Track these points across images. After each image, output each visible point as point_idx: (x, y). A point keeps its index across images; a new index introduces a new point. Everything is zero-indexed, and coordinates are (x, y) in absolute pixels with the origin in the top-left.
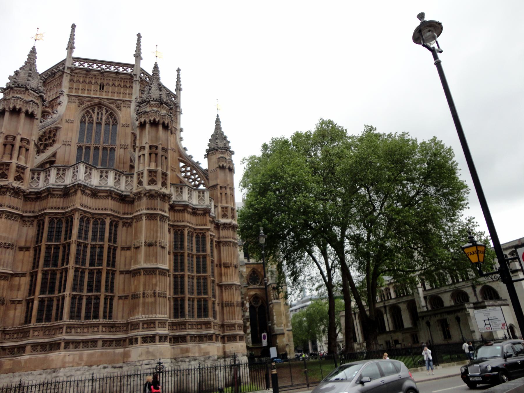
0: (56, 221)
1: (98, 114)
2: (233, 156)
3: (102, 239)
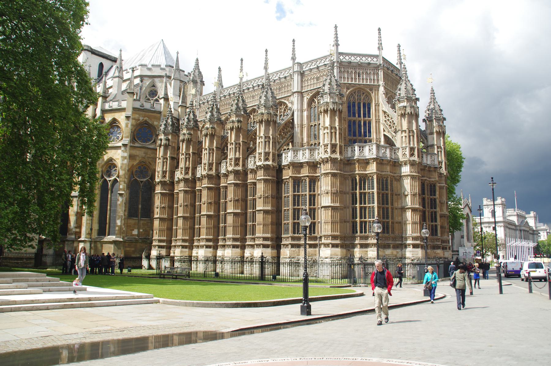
0: (362, 179)
1: (358, 95)
2: (444, 122)
3: (387, 190)
